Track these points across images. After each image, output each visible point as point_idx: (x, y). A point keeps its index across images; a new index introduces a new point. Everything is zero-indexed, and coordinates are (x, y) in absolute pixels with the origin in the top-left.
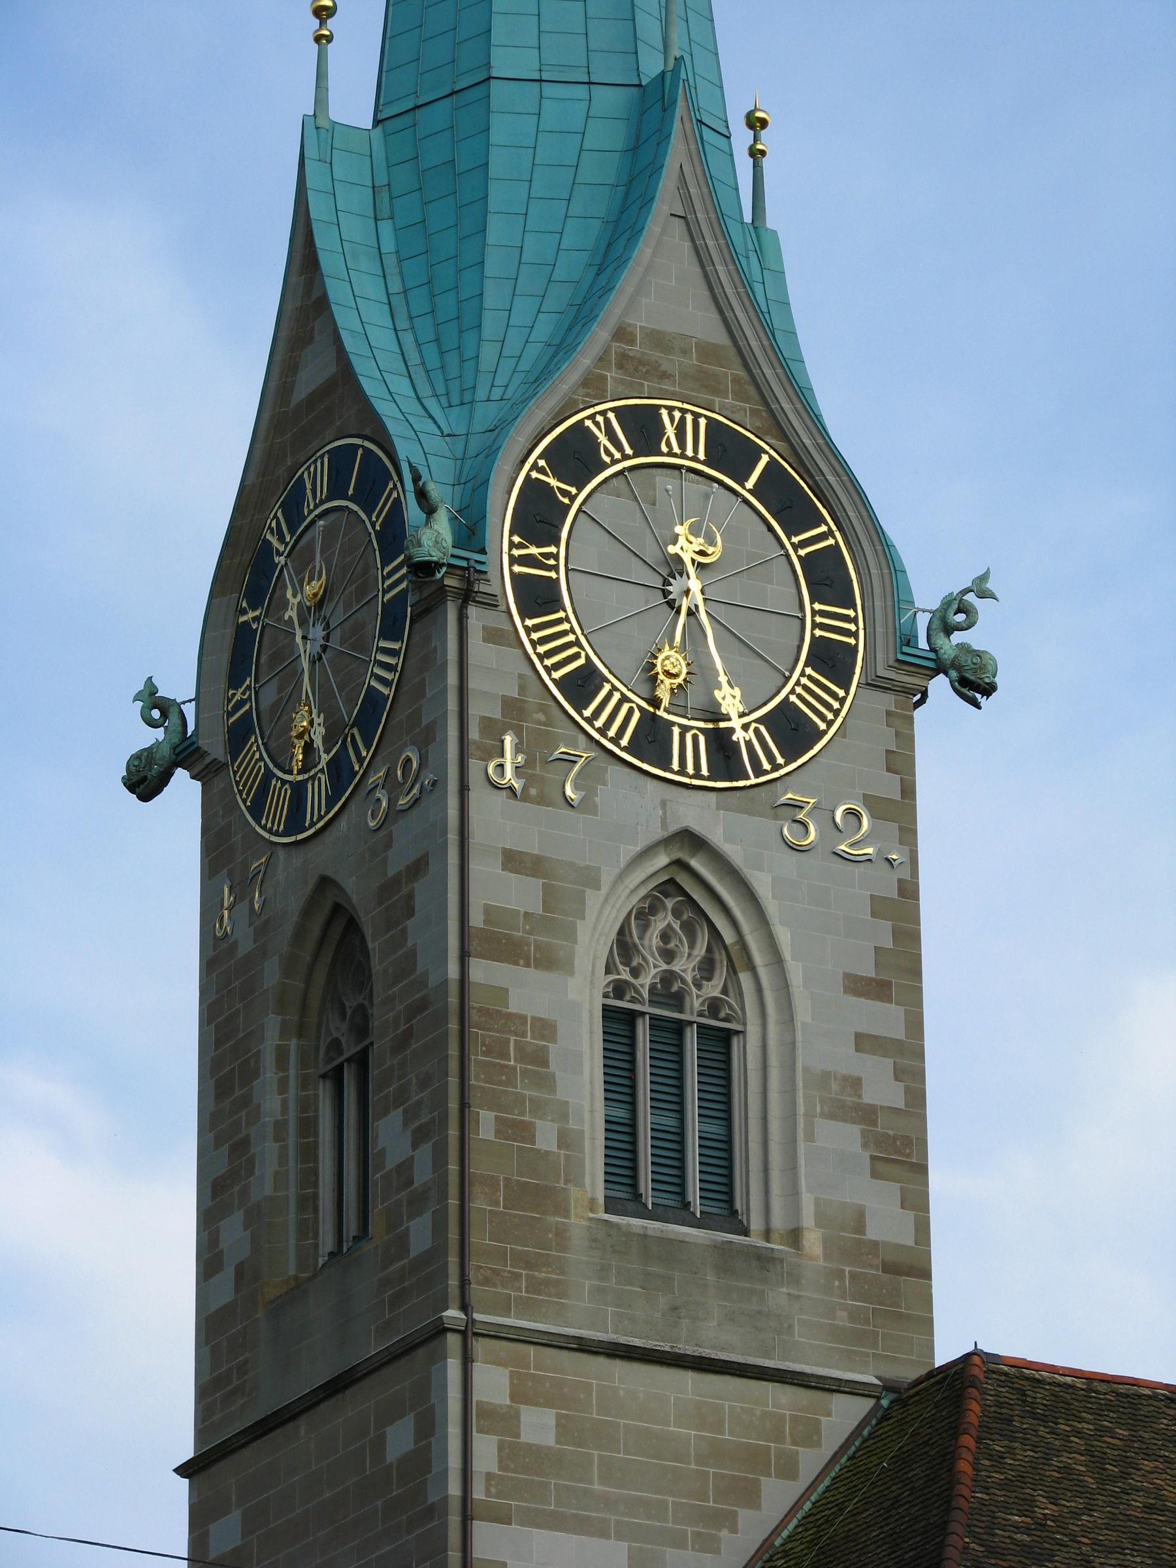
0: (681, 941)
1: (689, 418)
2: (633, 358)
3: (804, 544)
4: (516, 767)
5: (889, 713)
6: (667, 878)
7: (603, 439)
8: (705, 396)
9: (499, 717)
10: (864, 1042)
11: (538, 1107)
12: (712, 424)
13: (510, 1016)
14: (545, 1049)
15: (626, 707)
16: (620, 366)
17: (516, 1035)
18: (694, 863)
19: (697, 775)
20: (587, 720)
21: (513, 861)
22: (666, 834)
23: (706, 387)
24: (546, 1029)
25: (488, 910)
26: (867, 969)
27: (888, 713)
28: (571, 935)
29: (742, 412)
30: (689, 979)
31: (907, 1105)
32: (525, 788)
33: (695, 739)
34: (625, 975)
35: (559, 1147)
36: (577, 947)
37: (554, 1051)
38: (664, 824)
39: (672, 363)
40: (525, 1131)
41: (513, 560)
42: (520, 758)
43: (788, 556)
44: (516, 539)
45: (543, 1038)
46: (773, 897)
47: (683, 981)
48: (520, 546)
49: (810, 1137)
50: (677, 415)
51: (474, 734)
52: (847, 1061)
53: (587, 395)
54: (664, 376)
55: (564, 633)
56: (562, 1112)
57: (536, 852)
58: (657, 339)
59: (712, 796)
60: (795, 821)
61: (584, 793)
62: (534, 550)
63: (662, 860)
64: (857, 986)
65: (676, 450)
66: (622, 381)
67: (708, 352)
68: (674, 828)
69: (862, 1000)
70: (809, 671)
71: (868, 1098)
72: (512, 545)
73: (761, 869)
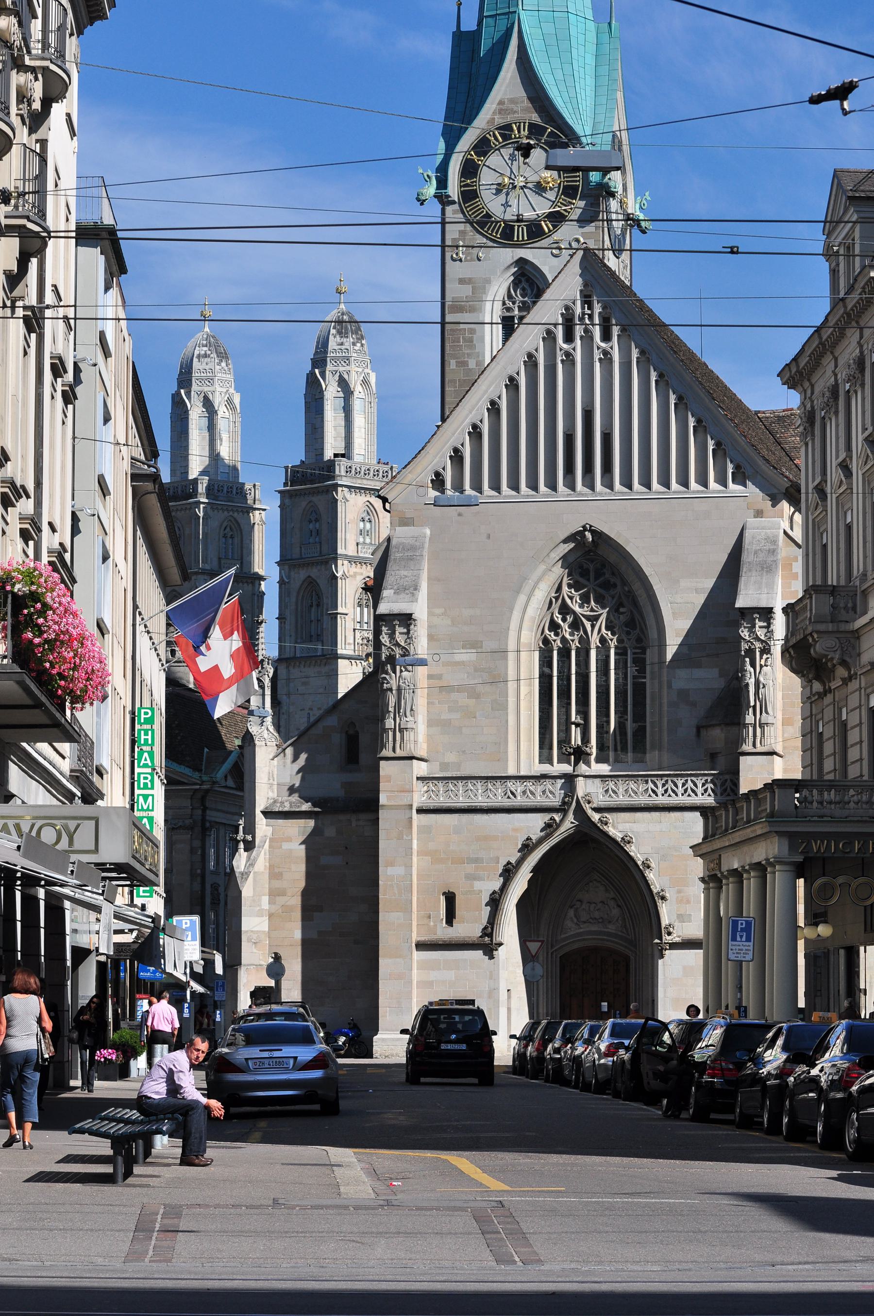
1: (522, 124)
16: (500, 113)
19: (523, 240)
20: (486, 232)
21: (462, 281)
32: (465, 258)
34: (509, 304)
38: (513, 258)
40: (464, 364)
44: (463, 179)
45: (471, 334)
48: (464, 181)
50: (518, 124)
54: (515, 112)
55: (479, 205)
58: (512, 101)
66: (500, 118)
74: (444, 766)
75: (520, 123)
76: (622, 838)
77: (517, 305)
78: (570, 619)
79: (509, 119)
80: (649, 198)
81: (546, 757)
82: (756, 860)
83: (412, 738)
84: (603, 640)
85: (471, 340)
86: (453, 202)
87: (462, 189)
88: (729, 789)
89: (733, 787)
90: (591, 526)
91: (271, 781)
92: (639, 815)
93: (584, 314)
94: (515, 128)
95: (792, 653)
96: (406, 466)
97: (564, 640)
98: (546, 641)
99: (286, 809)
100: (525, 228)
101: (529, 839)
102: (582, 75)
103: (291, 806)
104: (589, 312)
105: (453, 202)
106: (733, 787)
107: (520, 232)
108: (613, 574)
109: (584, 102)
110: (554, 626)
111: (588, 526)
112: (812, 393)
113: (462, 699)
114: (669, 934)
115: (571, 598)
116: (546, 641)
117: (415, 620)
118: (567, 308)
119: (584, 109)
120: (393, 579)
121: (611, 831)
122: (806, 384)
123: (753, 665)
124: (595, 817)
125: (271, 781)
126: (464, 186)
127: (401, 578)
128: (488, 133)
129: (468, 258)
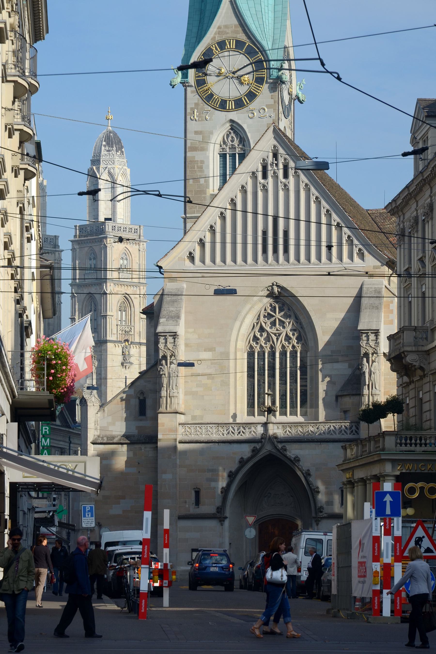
1: (232, 41)
12: (237, 41)
13: (195, 161)
16: (219, 34)
19: (232, 109)
24: (202, 162)
32: (198, 119)
33: (232, 102)
34: (224, 146)
37: (204, 166)
39: (229, 31)
44: (197, 73)
45: (202, 163)
48: (198, 74)
51: (188, 111)
54: (228, 33)
58: (226, 27)
65: (229, 47)
74: (194, 417)
75: (230, 40)
76: (295, 458)
77: (228, 147)
78: (265, 334)
79: (224, 37)
80: (304, 83)
81: (251, 413)
82: (374, 473)
83: (176, 402)
84: (283, 347)
85: (201, 168)
86: (191, 86)
87: (197, 78)
88: (354, 431)
89: (357, 430)
90: (277, 283)
91: (96, 425)
92: (304, 445)
93: (273, 163)
94: (228, 43)
95: (393, 361)
96: (172, 249)
97: (261, 347)
98: (251, 347)
99: (105, 441)
100: (233, 102)
101: (242, 458)
102: (267, 11)
103: (107, 440)
104: (276, 162)
105: (191, 86)
106: (357, 430)
107: (231, 105)
108: (289, 309)
109: (268, 27)
110: (255, 339)
111: (275, 284)
112: (404, 218)
113: (204, 380)
114: (321, 512)
115: (265, 323)
116: (251, 347)
117: (178, 335)
118: (264, 160)
119: (268, 31)
120: (165, 312)
121: (288, 454)
122: (400, 213)
123: (368, 361)
124: (280, 446)
125: (96, 425)
127: (170, 312)
128: (212, 46)
129: (200, 119)
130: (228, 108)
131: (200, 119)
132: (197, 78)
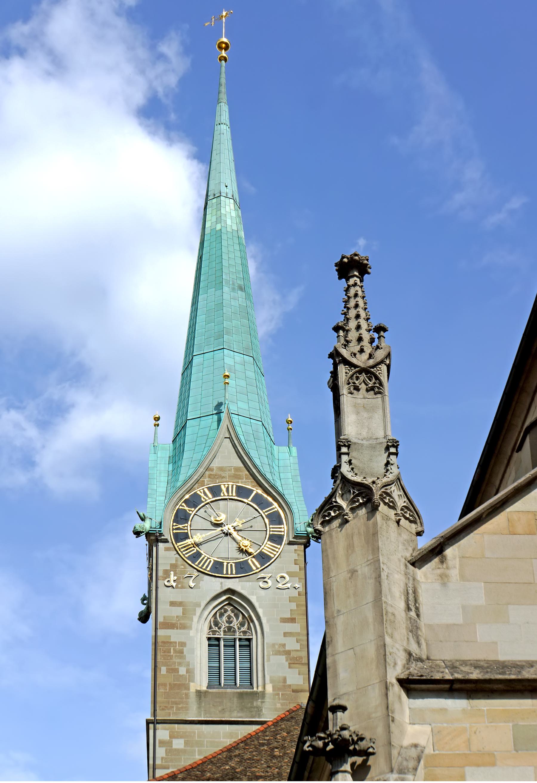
0: (233, 618)
2: (213, 475)
3: (266, 512)
4: (174, 581)
5: (295, 550)
6: (227, 602)
7: (202, 495)
8: (236, 480)
9: (169, 569)
10: (285, 634)
11: (180, 664)
13: (171, 643)
14: (183, 649)
15: (209, 560)
16: (209, 477)
17: (173, 646)
18: (234, 597)
19: (232, 574)
21: (172, 604)
22: (222, 590)
23: (236, 478)
24: (183, 644)
25: (164, 617)
26: (288, 616)
27: (295, 550)
28: (192, 620)
29: (248, 482)
30: (236, 627)
31: (300, 648)
33: (231, 565)
35: (187, 673)
36: (193, 623)
37: (185, 649)
38: (222, 587)
40: (177, 670)
41: (173, 529)
42: (175, 578)
43: (261, 516)
44: (175, 524)
45: (182, 646)
46: (257, 601)
47: (234, 628)
48: (176, 525)
49: (269, 660)
51: (160, 573)
52: (282, 640)
53: (198, 486)
56: (188, 664)
57: (180, 600)
58: (221, 469)
59: (238, 579)
60: (264, 582)
61: (195, 584)
62: (180, 526)
63: (224, 598)
64: (284, 620)
67: (237, 469)
68: (225, 588)
69: (286, 624)
70: (269, 543)
71: (287, 648)
72: (173, 526)
73: (253, 595)
85: (182, 652)
87: (175, 531)
100: (233, 565)
105: (166, 541)
126: (177, 529)
129: (180, 586)
130: (225, 572)
131: (180, 586)
132: (175, 531)
